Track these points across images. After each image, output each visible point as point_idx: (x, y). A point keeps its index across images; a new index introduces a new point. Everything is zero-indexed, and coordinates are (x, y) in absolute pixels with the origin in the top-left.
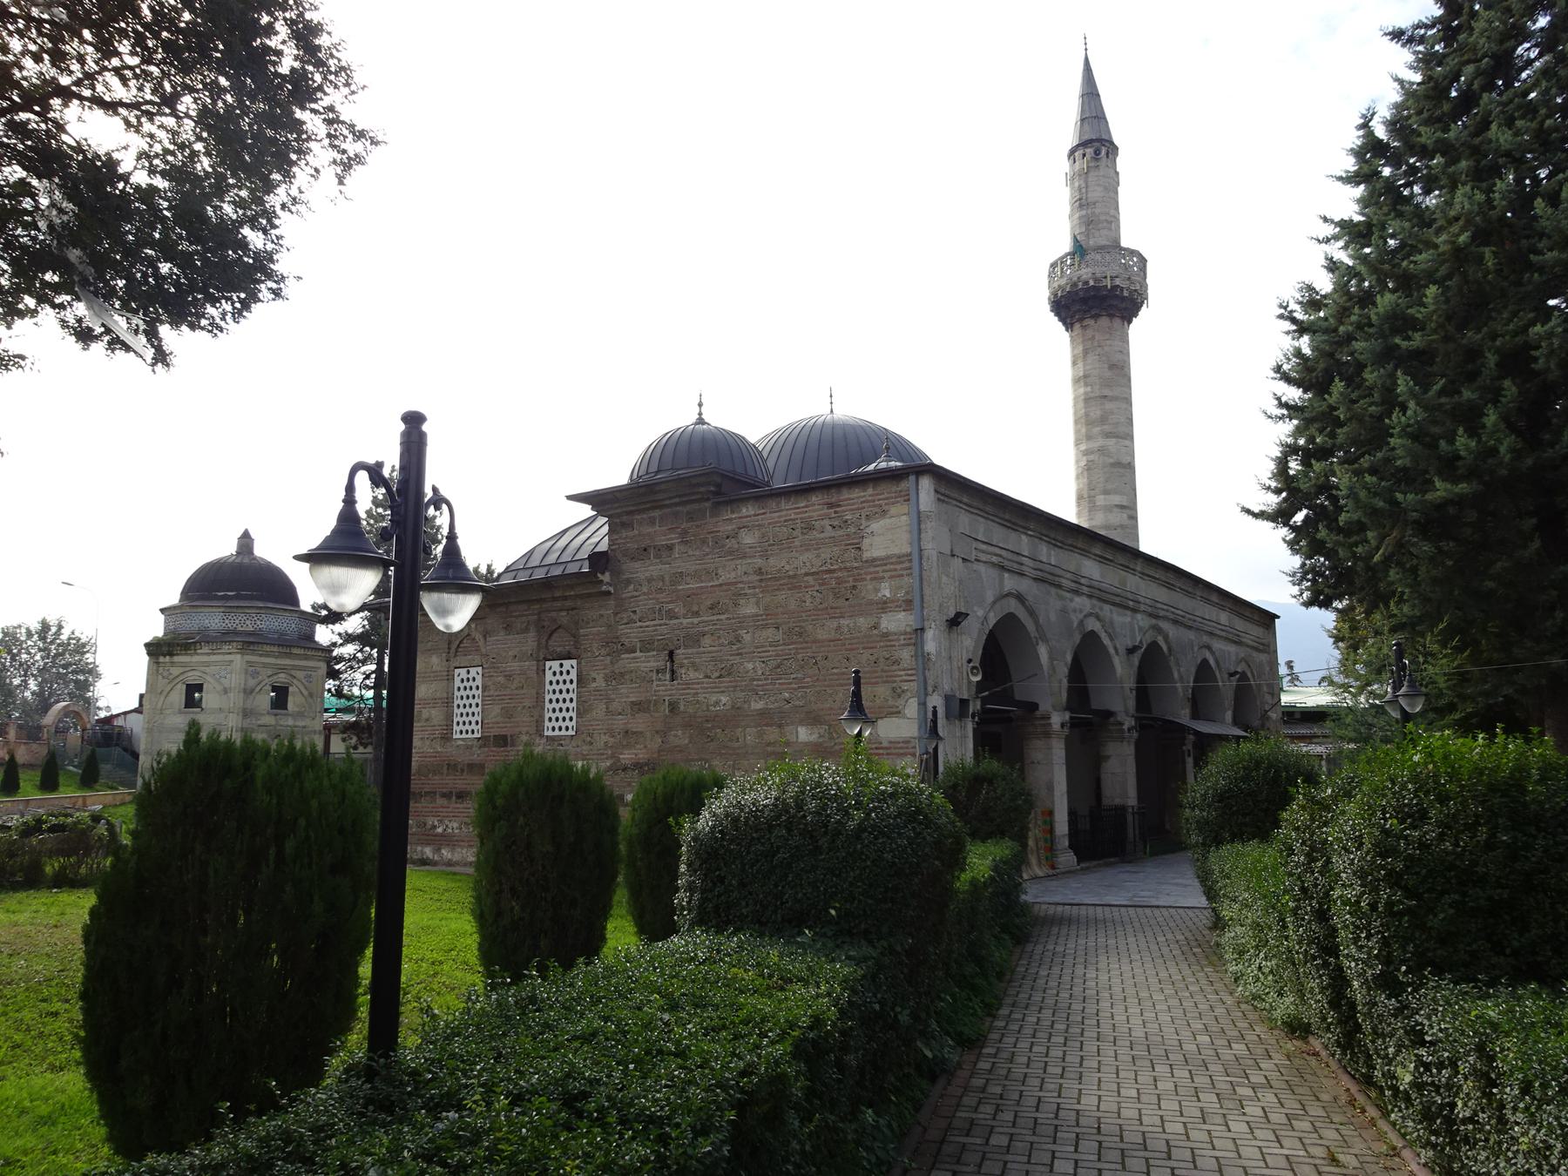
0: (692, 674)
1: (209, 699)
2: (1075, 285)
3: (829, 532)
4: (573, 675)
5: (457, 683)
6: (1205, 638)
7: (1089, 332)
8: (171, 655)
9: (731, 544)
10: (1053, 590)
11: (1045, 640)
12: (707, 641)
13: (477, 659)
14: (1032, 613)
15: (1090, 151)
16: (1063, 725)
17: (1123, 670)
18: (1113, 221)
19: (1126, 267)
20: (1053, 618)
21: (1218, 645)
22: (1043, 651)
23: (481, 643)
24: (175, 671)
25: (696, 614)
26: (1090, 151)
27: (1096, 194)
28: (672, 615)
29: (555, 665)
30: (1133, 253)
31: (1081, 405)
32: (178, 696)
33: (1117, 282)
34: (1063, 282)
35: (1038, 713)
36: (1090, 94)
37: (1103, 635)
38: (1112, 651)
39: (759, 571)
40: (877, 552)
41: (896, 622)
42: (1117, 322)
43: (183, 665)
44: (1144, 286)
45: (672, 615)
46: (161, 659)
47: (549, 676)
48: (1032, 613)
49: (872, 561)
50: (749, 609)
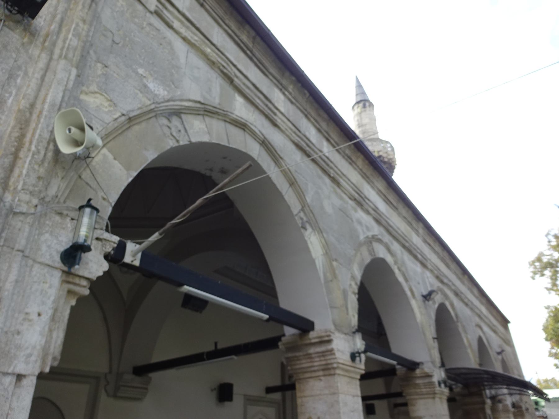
6: (477, 319)
10: (327, 180)
11: (319, 231)
14: (293, 183)
15: (361, 105)
16: (353, 357)
17: (423, 316)
19: (384, 148)
20: (329, 209)
21: (485, 328)
22: (314, 243)
26: (361, 105)
27: (366, 121)
30: (387, 142)
33: (381, 154)
35: (312, 334)
37: (396, 271)
38: (409, 293)
44: (394, 158)
48: (293, 183)
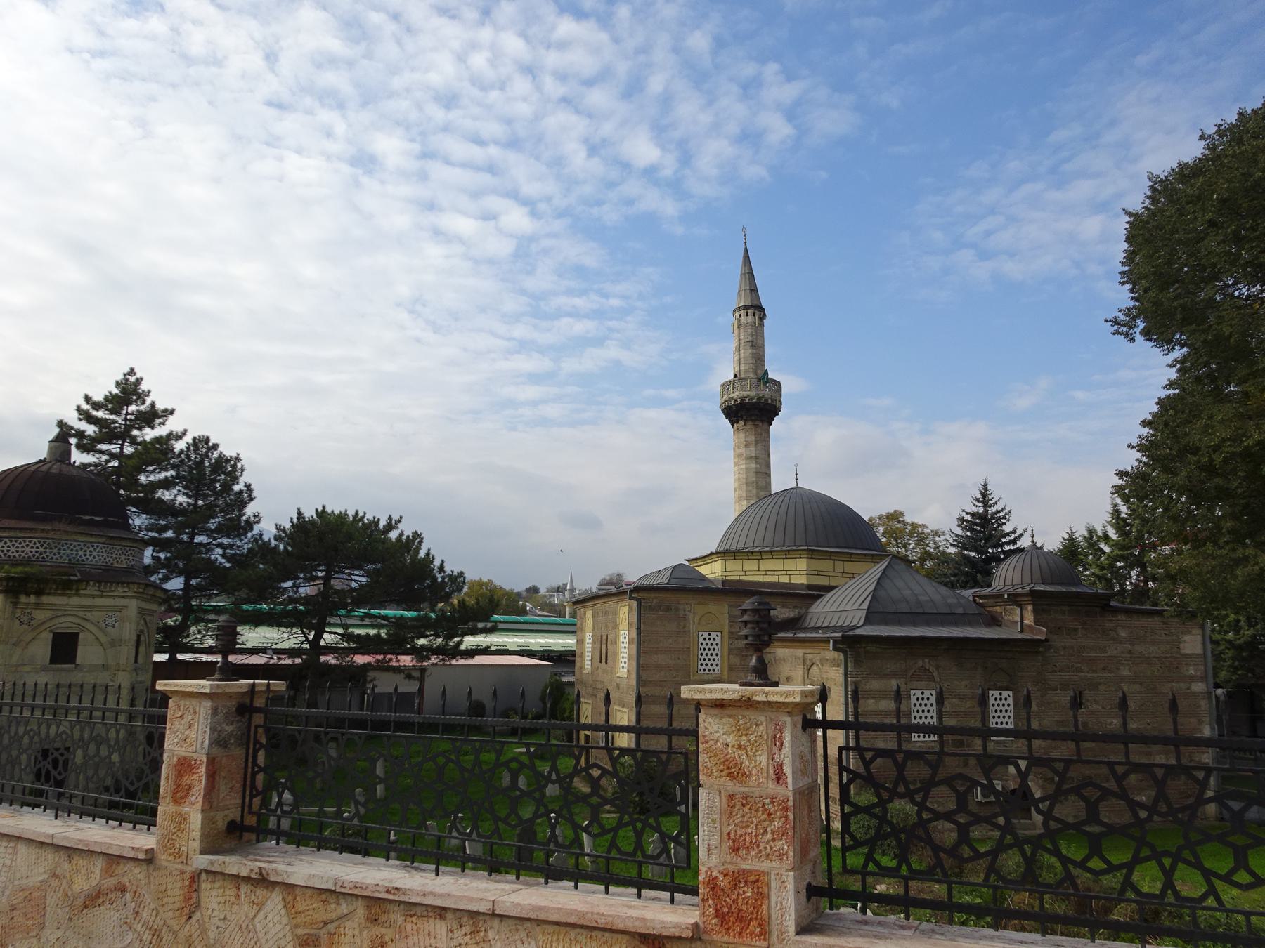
0: (1095, 706)
1: (87, 653)
2: (759, 399)
3: (1164, 637)
4: (1010, 701)
5: (913, 700)
7: (759, 430)
8: (39, 593)
9: (1113, 634)
12: (1102, 687)
13: (932, 684)
18: (759, 359)
23: (935, 674)
24: (40, 615)
25: (1094, 671)
28: (1080, 671)
29: (996, 694)
31: (752, 474)
32: (42, 649)
34: (753, 394)
36: (749, 274)
39: (1130, 652)
40: (1187, 651)
41: (1199, 687)
42: (766, 424)
43: (54, 608)
45: (1080, 671)
46: (23, 599)
47: (992, 701)
49: (1186, 656)
50: (1125, 672)
